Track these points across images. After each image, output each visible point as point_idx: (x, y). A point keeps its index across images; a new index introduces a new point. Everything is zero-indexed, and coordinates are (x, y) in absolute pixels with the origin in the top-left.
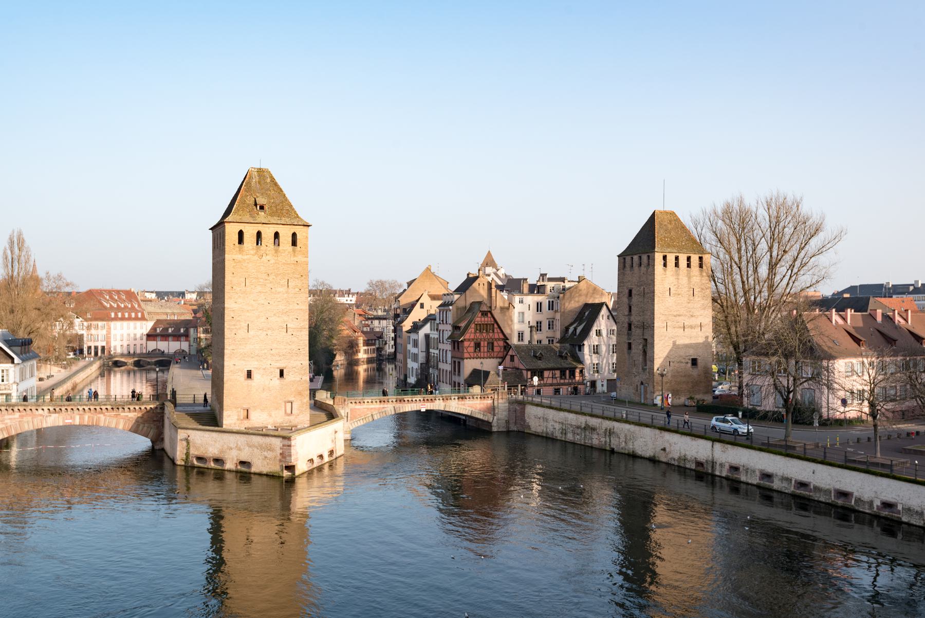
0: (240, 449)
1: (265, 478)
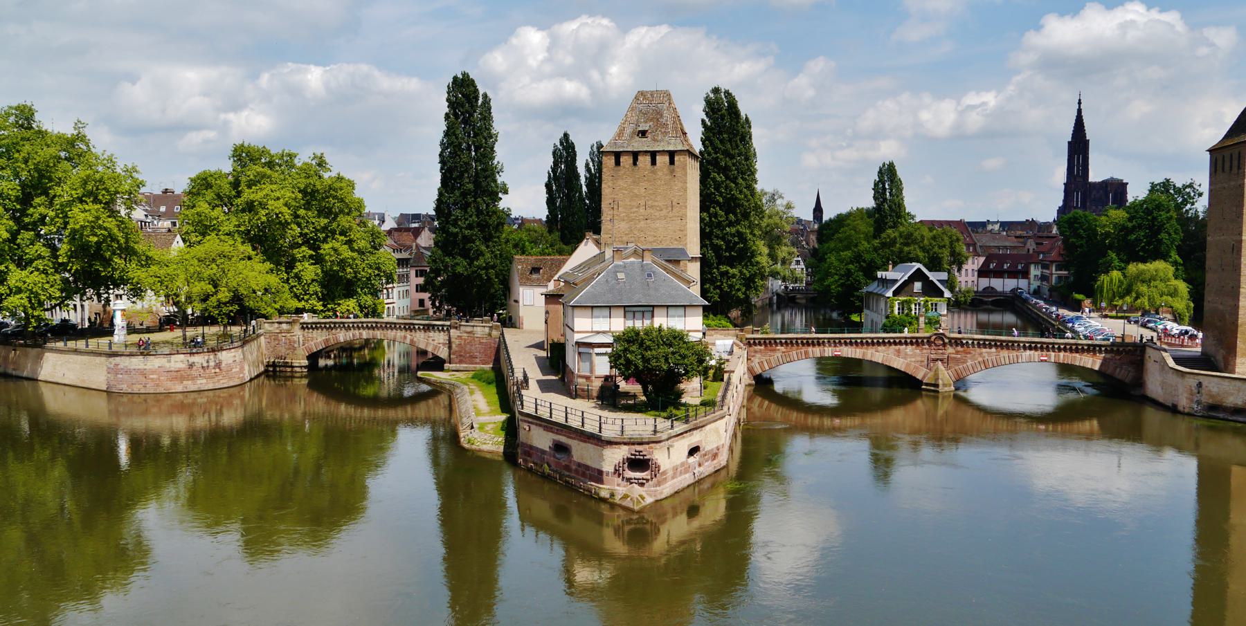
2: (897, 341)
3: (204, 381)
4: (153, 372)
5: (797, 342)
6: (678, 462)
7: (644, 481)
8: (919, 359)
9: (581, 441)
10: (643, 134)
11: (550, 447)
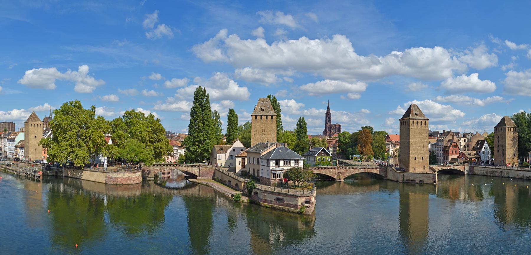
0: (419, 177)
1: (428, 185)
3: (133, 181)
4: (120, 178)
9: (288, 197)
10: (263, 110)
11: (275, 200)
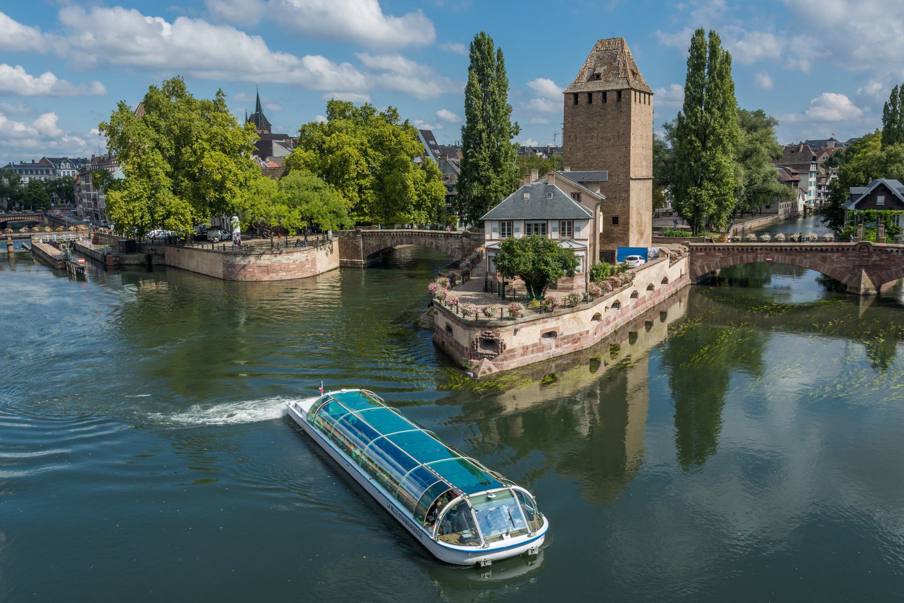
2: (824, 249)
3: (284, 274)
5: (733, 249)
6: (530, 343)
7: (493, 357)
8: (845, 265)
10: (598, 77)
